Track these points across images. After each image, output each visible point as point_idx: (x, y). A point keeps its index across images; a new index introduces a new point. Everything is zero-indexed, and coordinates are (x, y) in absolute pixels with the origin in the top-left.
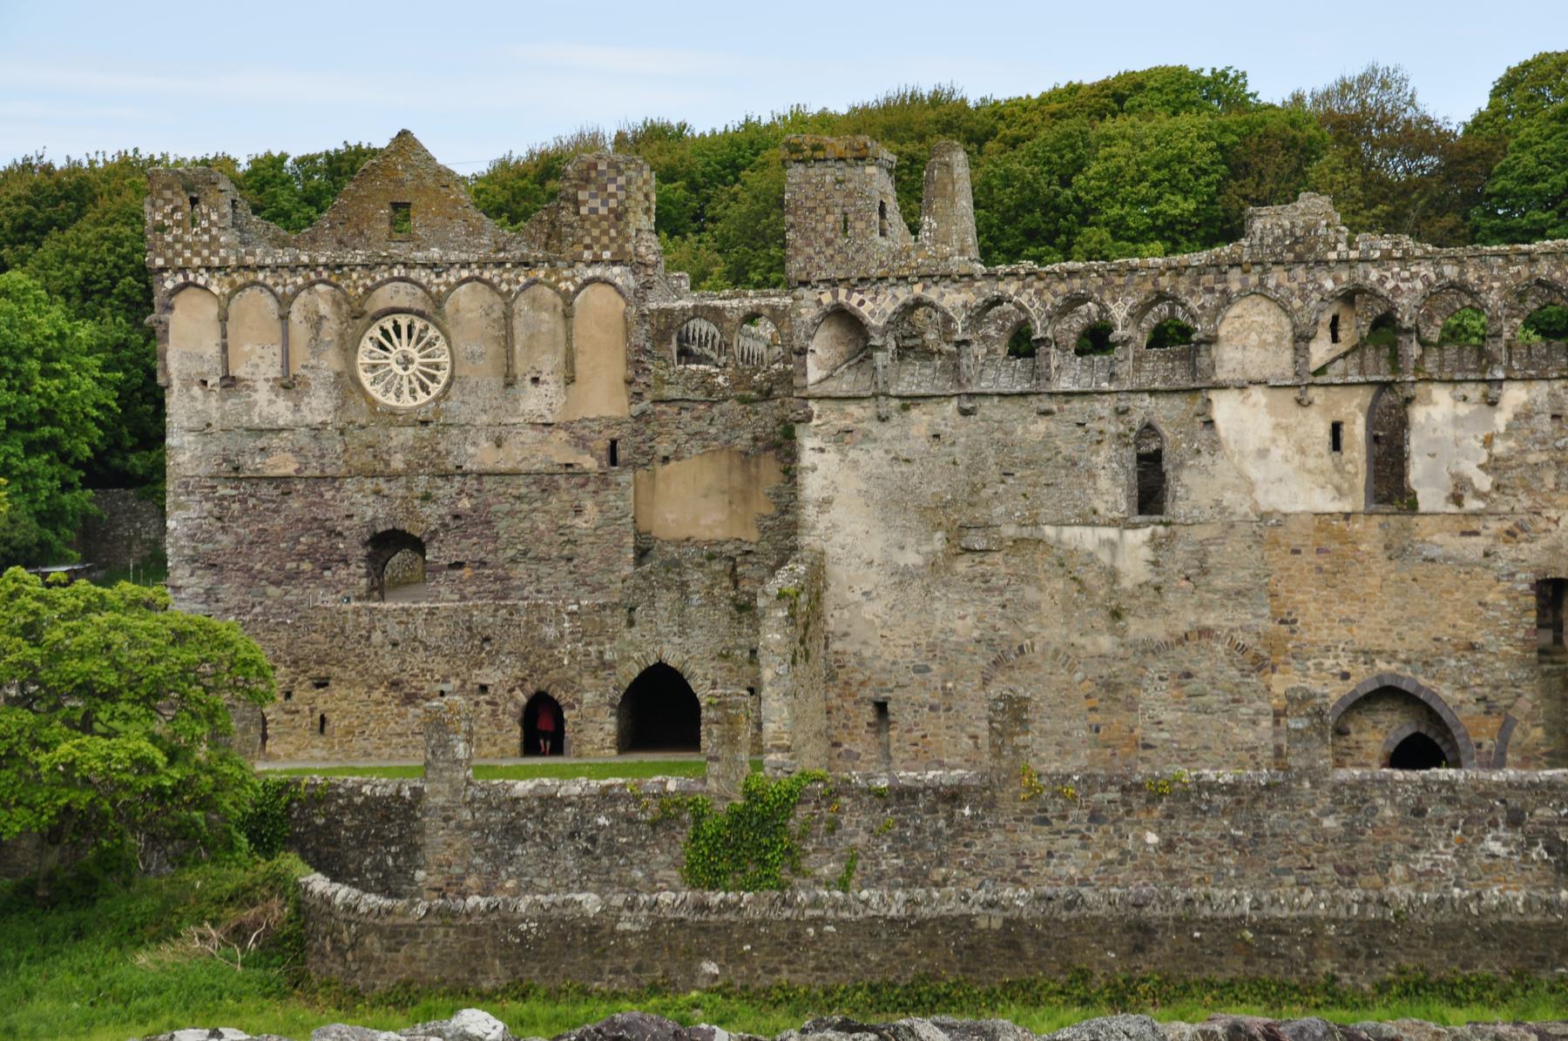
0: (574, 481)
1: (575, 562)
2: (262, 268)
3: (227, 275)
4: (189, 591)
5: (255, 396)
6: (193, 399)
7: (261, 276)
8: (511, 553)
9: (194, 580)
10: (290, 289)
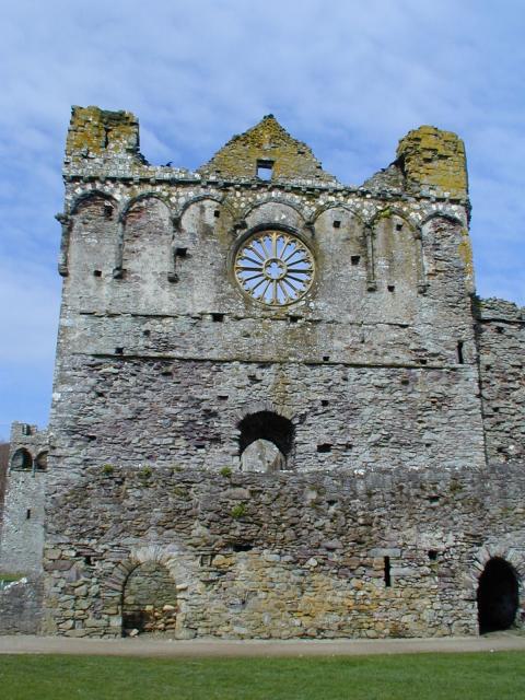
0: (432, 373)
1: (434, 446)
2: (160, 182)
3: (129, 186)
4: (68, 461)
5: (143, 286)
6: (88, 286)
7: (158, 189)
8: (378, 436)
9: (73, 451)
10: (182, 201)
